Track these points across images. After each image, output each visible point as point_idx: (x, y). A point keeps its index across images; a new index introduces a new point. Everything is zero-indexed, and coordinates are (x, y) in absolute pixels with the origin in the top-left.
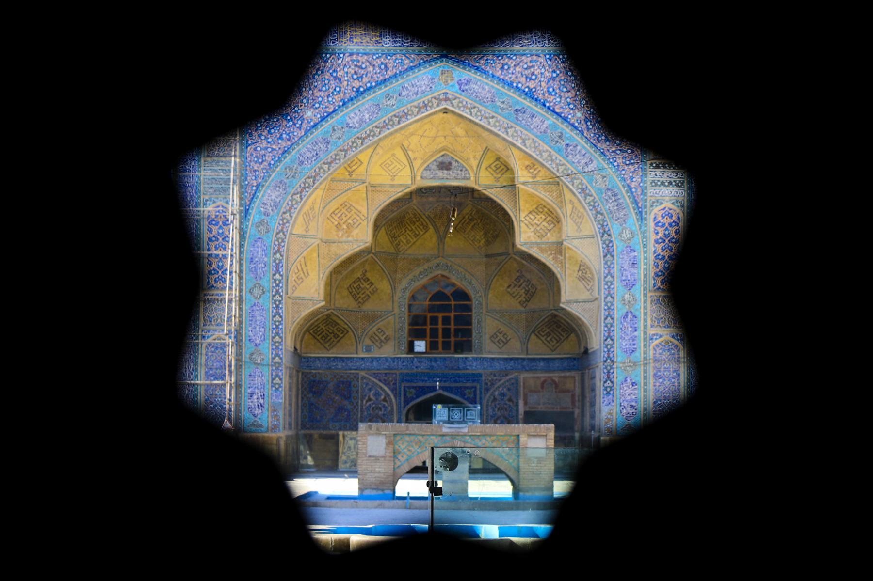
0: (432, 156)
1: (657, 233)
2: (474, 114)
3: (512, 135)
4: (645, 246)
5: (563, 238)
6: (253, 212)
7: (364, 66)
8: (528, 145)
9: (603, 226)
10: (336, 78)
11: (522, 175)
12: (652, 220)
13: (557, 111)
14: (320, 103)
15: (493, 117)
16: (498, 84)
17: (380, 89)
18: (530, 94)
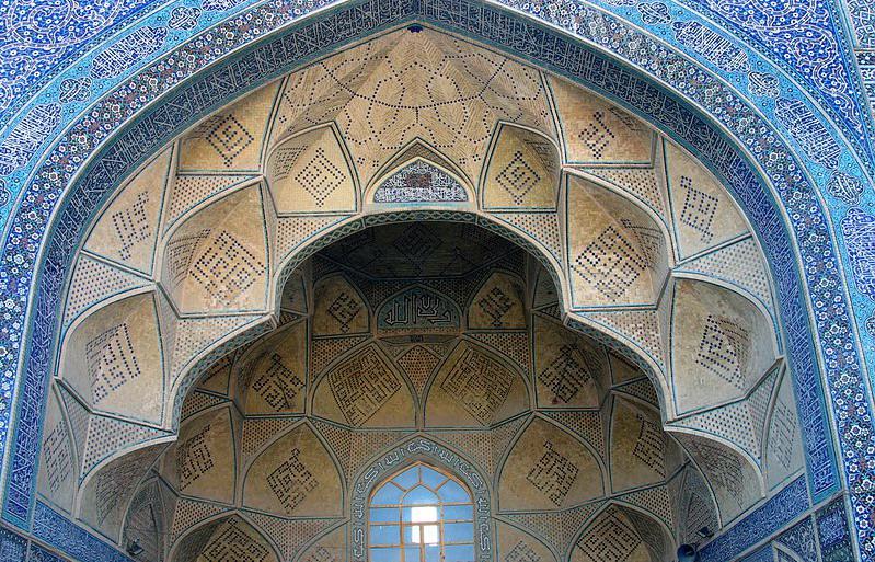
3: (558, 15)
5: (671, 266)
8: (593, 32)
9: (785, 173)
11: (574, 153)
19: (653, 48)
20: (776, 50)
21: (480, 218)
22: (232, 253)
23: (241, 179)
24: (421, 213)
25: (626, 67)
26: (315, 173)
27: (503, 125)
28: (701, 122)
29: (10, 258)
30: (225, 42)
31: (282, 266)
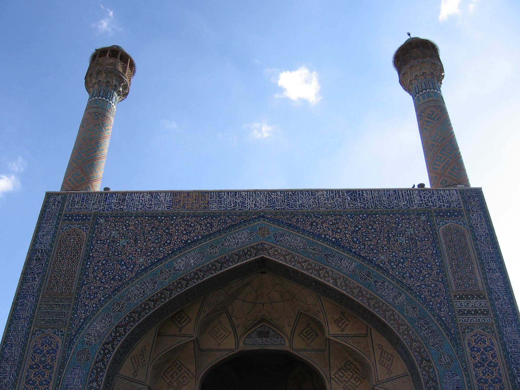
0: (254, 326)
1: (474, 358)
2: (288, 260)
3: (324, 276)
4: (466, 370)
5: (374, 383)
6: (77, 342)
7: (192, 225)
8: (339, 284)
9: (419, 353)
10: (168, 234)
11: (332, 330)
12: (466, 345)
13: (363, 255)
14: (152, 252)
15: (306, 261)
16: (308, 236)
17: (206, 241)
18: (337, 243)
19: (364, 293)
20: (418, 294)
21: (291, 353)
22: (180, 369)
23: (186, 338)
24: (265, 350)
25: (353, 301)
26: (218, 331)
27: (301, 313)
28: (385, 325)
29: (91, 384)
30: (182, 286)
31: (202, 375)
